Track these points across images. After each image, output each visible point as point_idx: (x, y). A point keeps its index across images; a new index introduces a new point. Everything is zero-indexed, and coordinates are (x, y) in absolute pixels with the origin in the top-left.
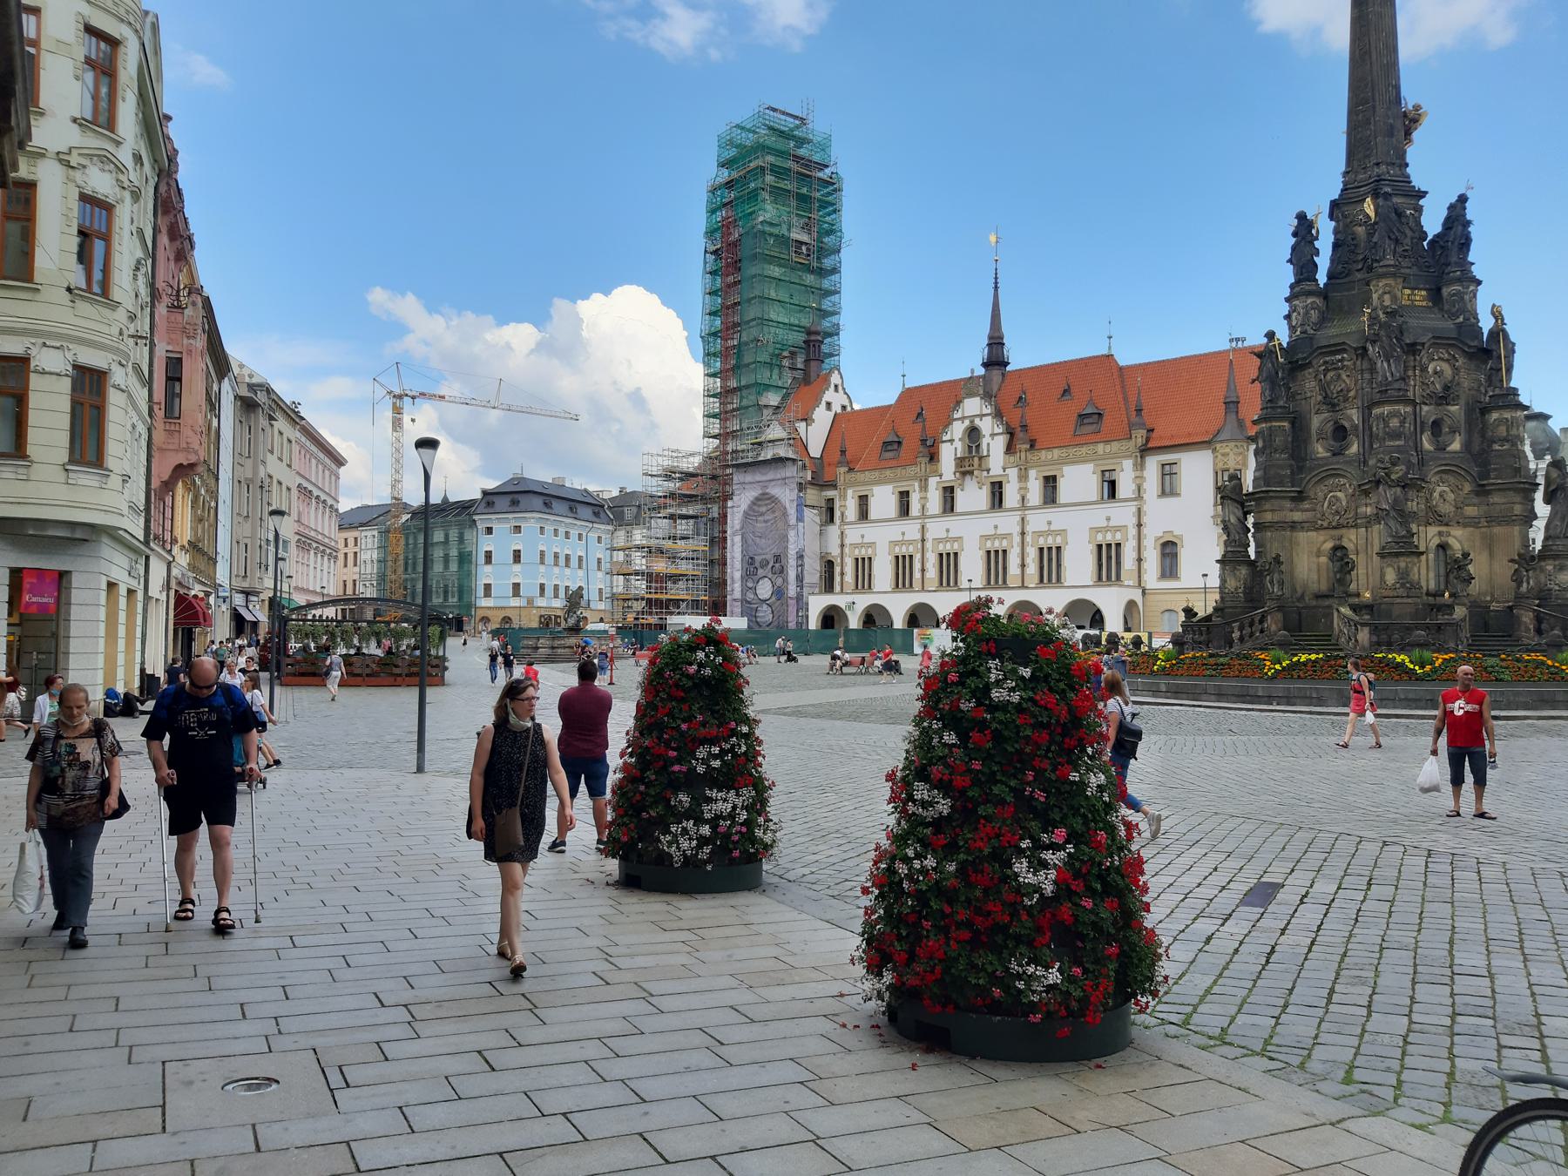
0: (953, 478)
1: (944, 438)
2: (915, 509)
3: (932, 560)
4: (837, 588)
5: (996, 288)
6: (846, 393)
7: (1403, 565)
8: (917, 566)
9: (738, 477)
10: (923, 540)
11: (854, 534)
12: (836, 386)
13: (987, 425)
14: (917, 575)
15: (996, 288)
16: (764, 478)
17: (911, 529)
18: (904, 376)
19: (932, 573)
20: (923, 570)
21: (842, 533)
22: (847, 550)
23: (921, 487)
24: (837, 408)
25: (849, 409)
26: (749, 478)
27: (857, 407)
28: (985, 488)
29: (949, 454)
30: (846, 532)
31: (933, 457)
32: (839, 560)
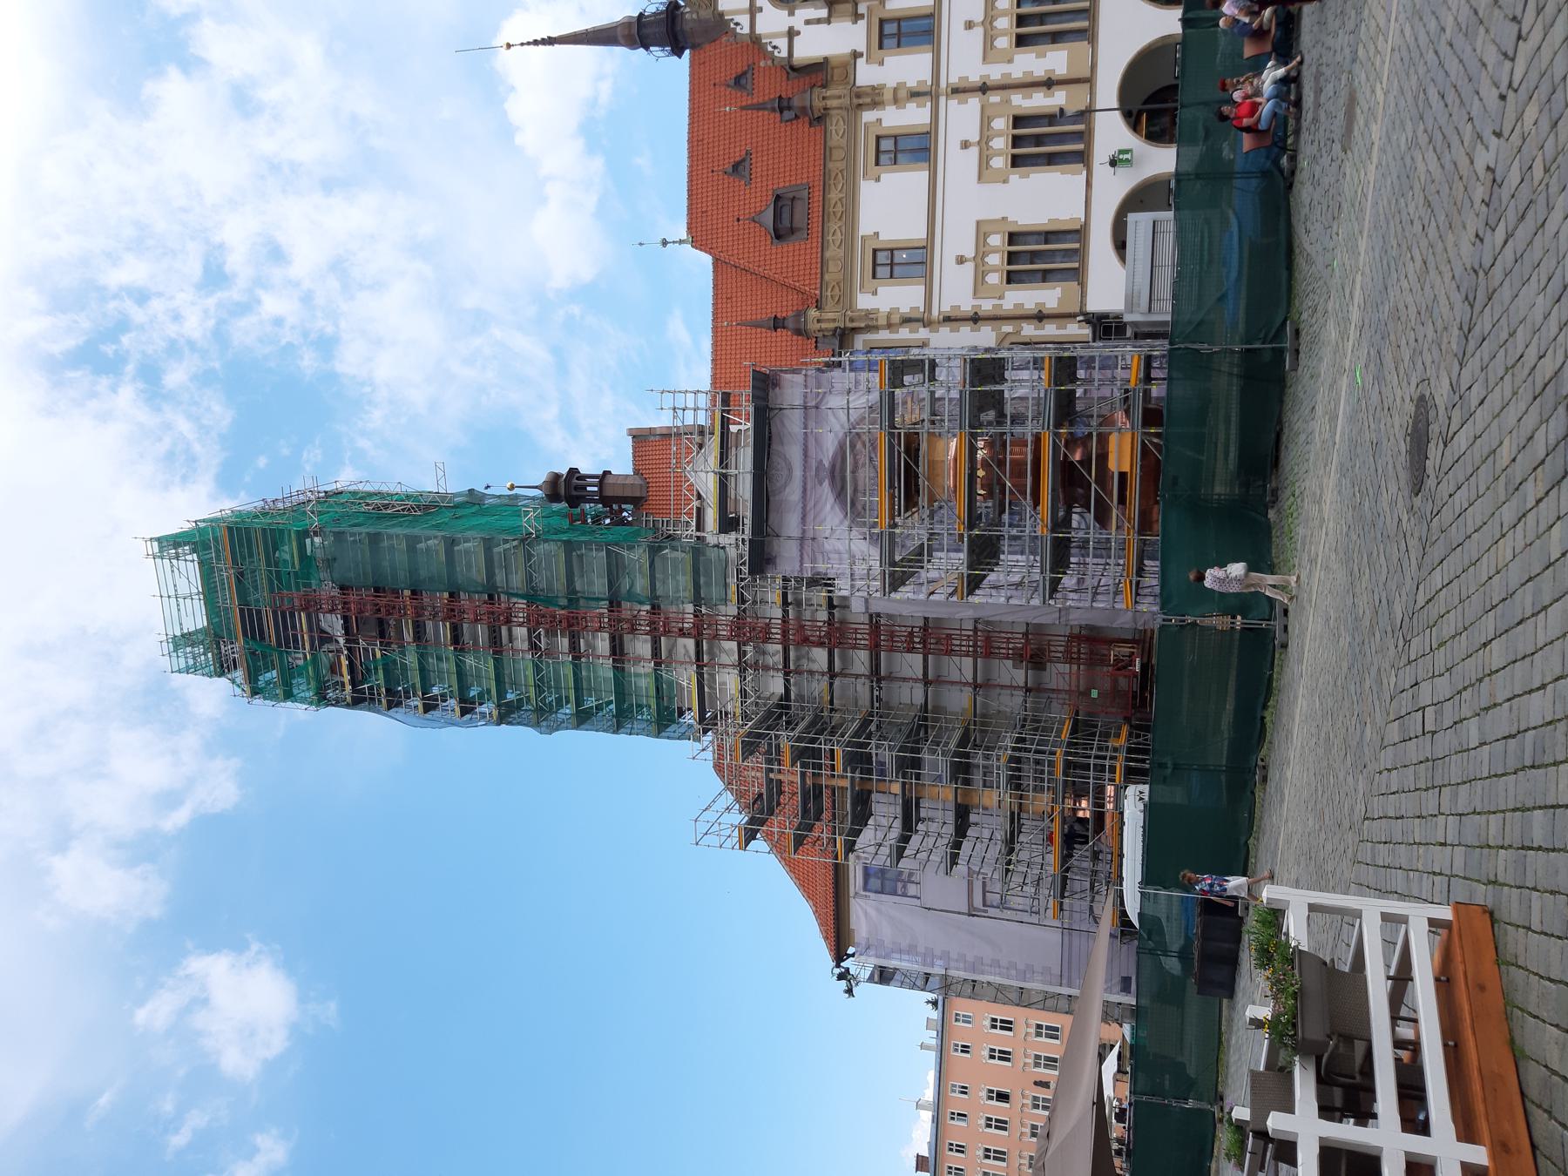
0: (862, 24)
1: (784, 54)
2: (913, 116)
5: (550, 41)
8: (1039, 102)
9: (789, 560)
10: (984, 89)
14: (1058, 99)
15: (550, 41)
16: (798, 473)
18: (665, 243)
19: (1056, 60)
20: (1049, 84)
21: (948, 319)
22: (987, 306)
23: (876, 104)
26: (791, 524)
30: (946, 308)
31: (818, 72)
32: (1007, 328)
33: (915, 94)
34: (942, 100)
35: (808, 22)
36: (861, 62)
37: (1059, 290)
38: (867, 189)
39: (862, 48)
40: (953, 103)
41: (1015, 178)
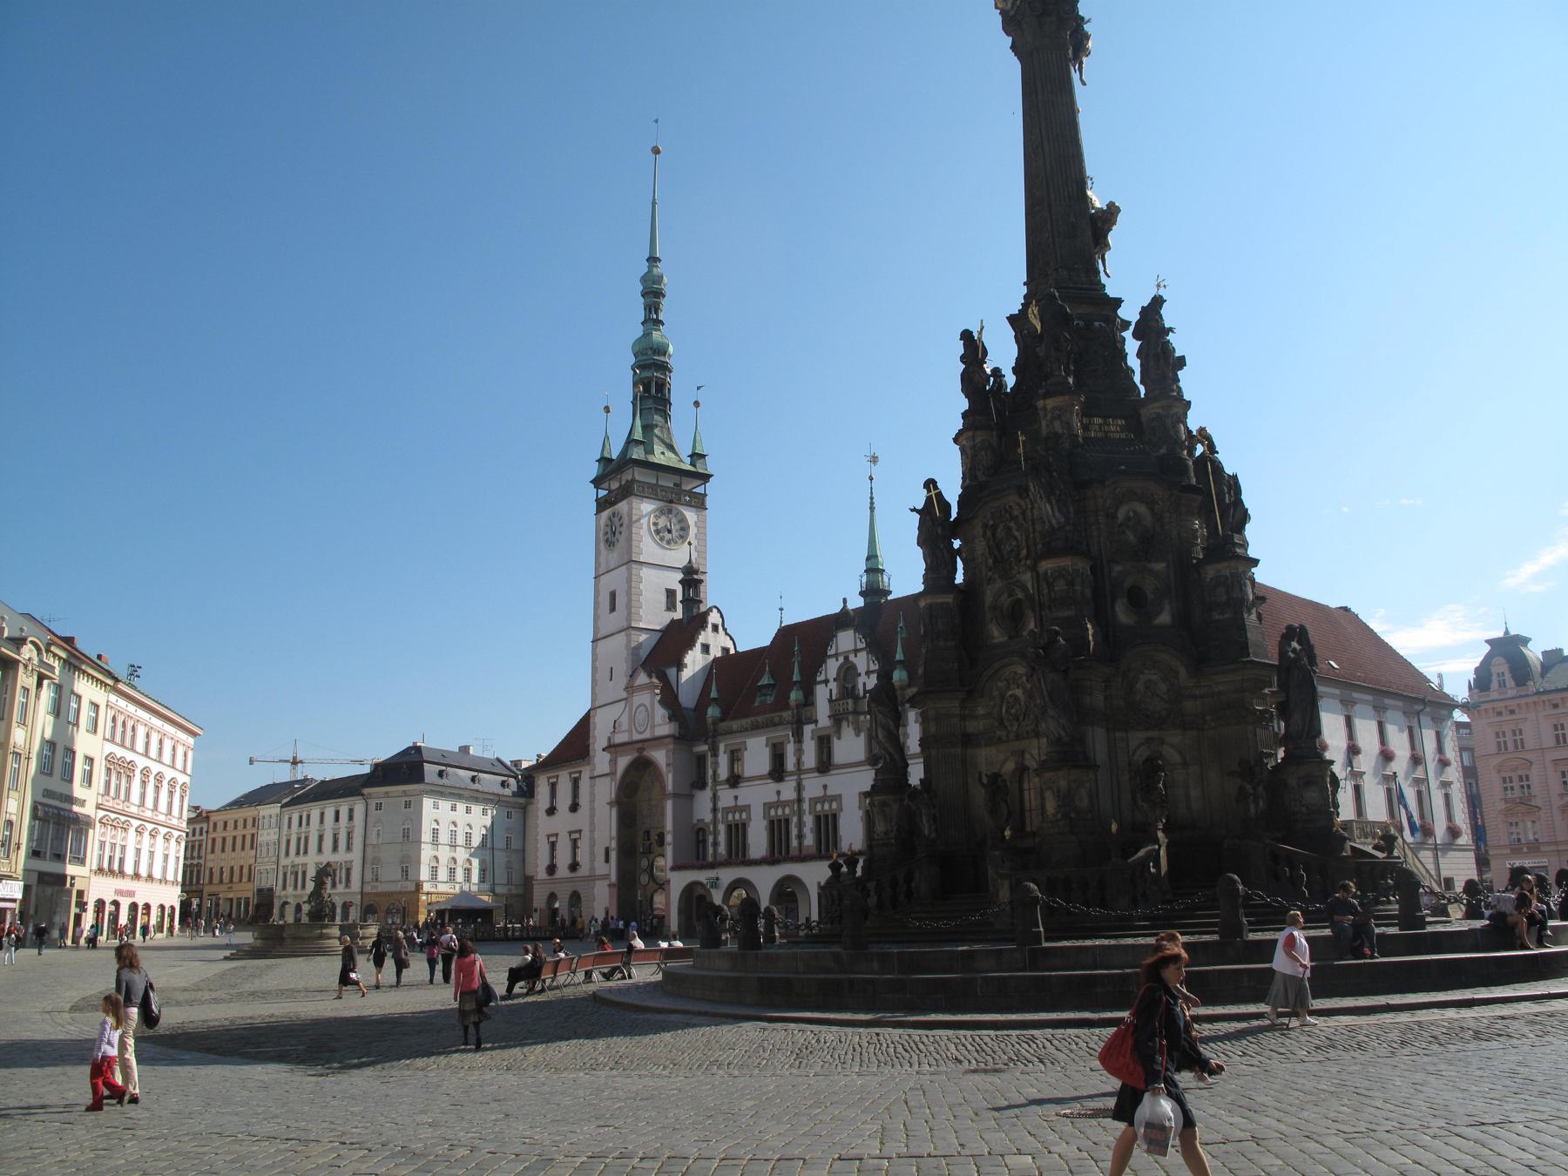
3: (809, 820)
4: (710, 859)
5: (872, 509)
6: (727, 634)
7: (1063, 784)
8: (794, 831)
10: (800, 800)
11: (726, 797)
12: (715, 628)
13: (862, 662)
14: (794, 843)
15: (872, 509)
17: (788, 790)
19: (809, 840)
22: (720, 816)
24: (716, 652)
25: (732, 651)
27: (740, 649)
28: (862, 735)
29: (822, 694)
32: (711, 827)
33: (799, 761)
34: (795, 777)
35: (831, 690)
36: (812, 726)
37: (724, 852)
38: (762, 740)
39: (820, 725)
40: (794, 784)
41: (765, 823)
